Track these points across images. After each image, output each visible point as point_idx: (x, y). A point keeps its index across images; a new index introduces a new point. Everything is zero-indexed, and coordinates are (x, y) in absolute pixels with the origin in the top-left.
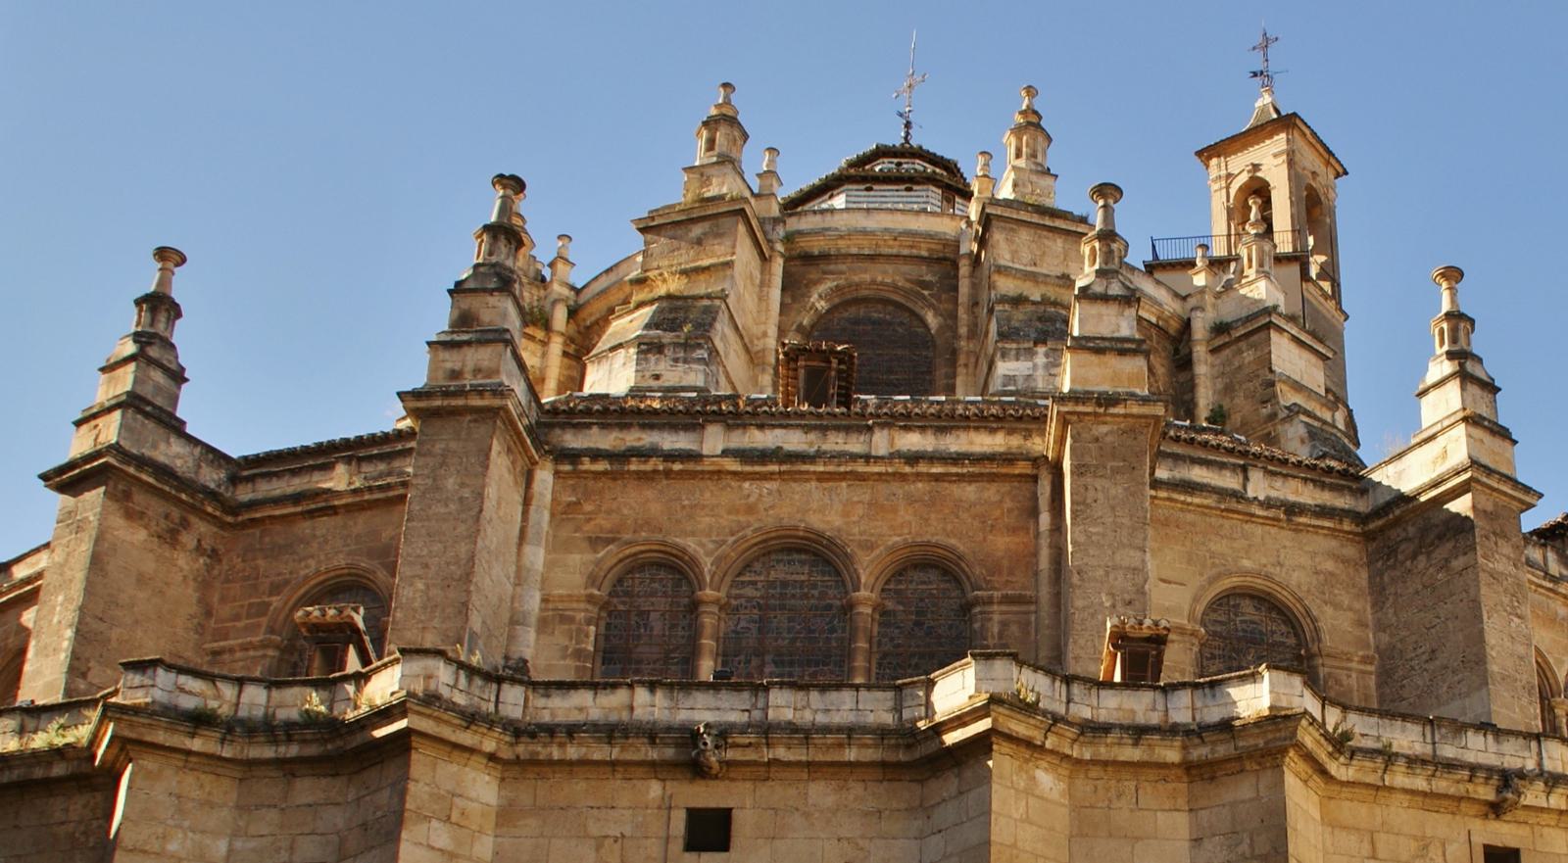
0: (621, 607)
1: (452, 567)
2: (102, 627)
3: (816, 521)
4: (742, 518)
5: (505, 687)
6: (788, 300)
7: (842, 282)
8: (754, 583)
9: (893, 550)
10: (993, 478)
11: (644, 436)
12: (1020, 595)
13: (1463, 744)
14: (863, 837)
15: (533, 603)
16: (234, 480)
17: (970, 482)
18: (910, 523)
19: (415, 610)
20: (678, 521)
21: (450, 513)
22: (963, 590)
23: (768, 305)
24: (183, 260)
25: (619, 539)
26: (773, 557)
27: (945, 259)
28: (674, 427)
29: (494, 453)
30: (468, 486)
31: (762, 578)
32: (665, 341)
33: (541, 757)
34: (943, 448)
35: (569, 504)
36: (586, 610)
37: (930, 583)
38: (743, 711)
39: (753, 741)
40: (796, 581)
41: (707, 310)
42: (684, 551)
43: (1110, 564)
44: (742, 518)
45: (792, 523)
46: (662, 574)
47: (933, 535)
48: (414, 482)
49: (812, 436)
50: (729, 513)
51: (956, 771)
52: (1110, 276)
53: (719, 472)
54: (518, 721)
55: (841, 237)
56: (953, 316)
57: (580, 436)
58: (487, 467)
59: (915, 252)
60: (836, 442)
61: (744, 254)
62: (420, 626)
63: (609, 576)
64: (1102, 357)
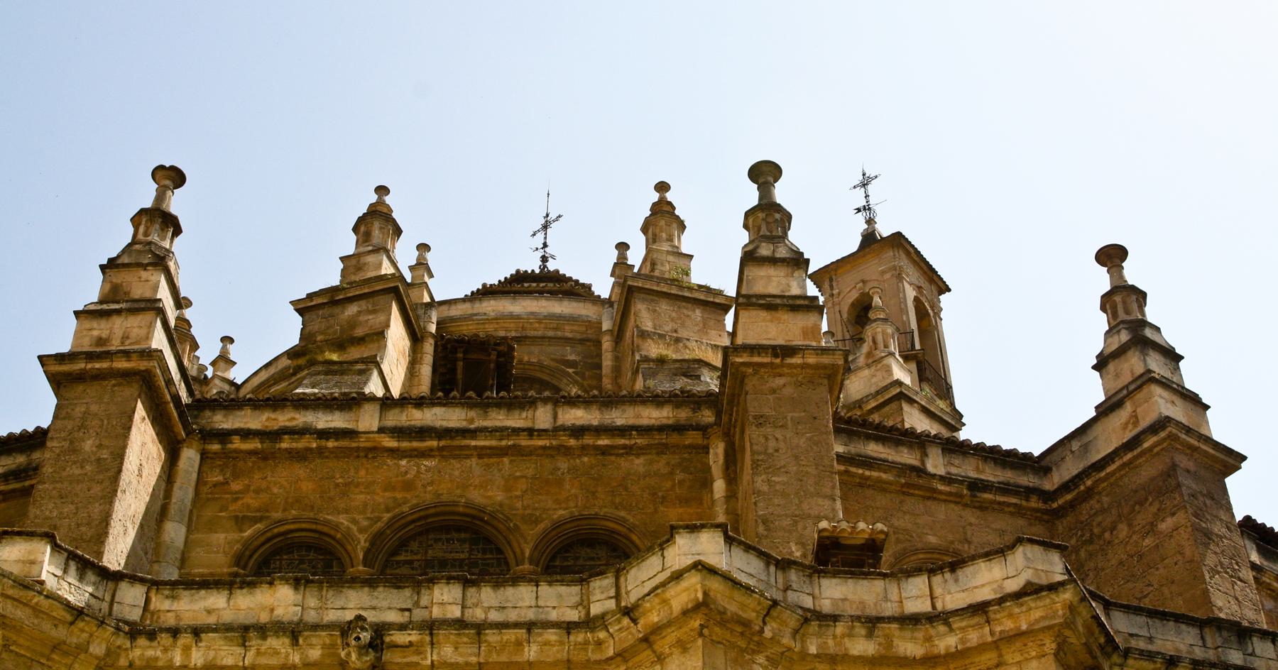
3: (476, 496)
4: (399, 495)
5: (124, 585)
8: (410, 562)
9: (558, 525)
10: (663, 449)
11: (297, 416)
17: (638, 456)
18: (576, 496)
20: (331, 499)
21: (86, 474)
25: (268, 518)
26: (431, 536)
27: (589, 340)
30: (108, 447)
31: (419, 557)
34: (609, 421)
37: (599, 559)
40: (455, 560)
42: (337, 527)
43: (797, 512)
44: (399, 495)
45: (452, 499)
46: (312, 555)
47: (601, 508)
49: (472, 414)
50: (385, 490)
52: (776, 241)
53: (374, 449)
59: (559, 334)
60: (499, 419)
63: (255, 557)
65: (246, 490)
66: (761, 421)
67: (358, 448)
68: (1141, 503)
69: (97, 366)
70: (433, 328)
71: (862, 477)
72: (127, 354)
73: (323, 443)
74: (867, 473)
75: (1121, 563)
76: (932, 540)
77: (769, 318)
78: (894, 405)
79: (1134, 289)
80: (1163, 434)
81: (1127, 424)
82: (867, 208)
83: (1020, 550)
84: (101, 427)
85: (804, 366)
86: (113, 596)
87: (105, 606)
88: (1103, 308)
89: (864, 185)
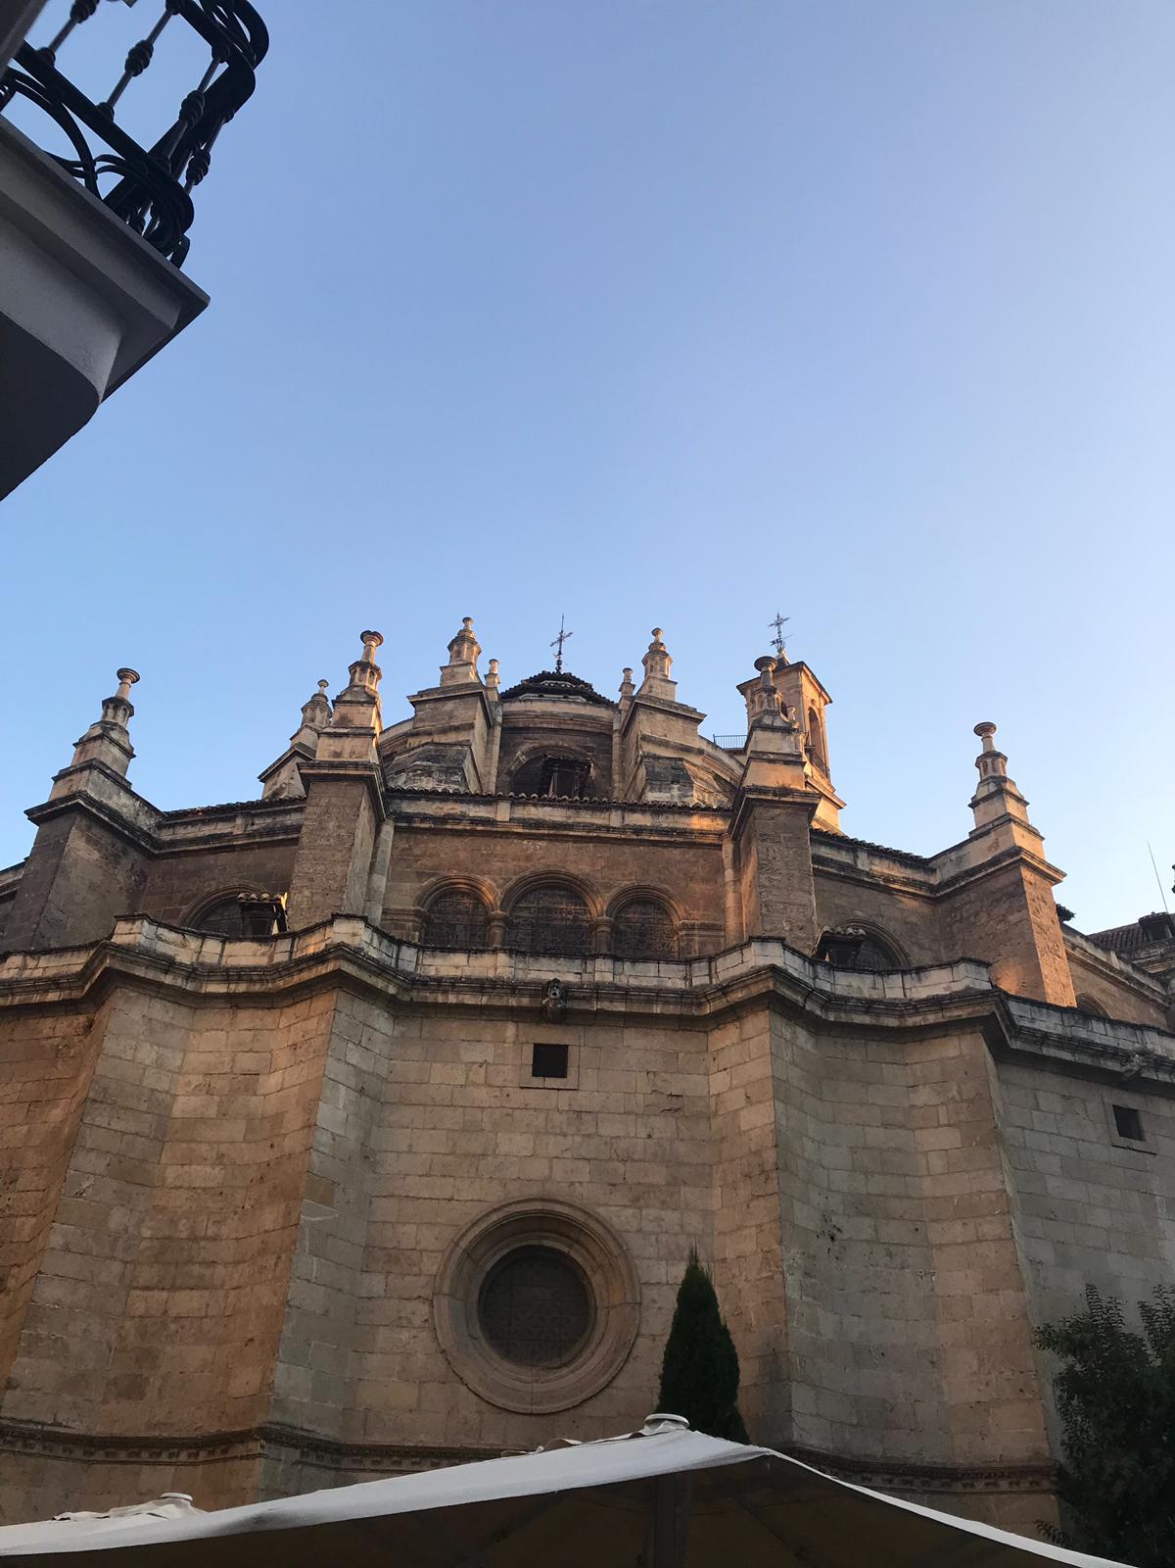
0: (436, 921)
1: (331, 882)
2: (62, 917)
3: (573, 869)
6: (502, 755)
7: (537, 745)
8: (529, 908)
9: (625, 892)
11: (456, 807)
12: (714, 925)
14: (666, 1072)
16: (159, 826)
17: (676, 848)
19: (302, 910)
22: (671, 921)
23: (491, 755)
26: (542, 892)
29: (362, 808)
30: (343, 827)
31: (534, 905)
32: (433, 769)
33: (429, 1001)
36: (414, 921)
37: (649, 914)
41: (459, 752)
44: (522, 864)
48: (306, 823)
49: (570, 813)
50: (513, 860)
51: (738, 1024)
54: (412, 973)
55: (537, 717)
56: (610, 769)
57: (413, 805)
58: (358, 816)
59: (583, 728)
60: (586, 817)
61: (480, 722)
63: (430, 899)
64: (772, 765)
65: (424, 855)
66: (764, 837)
67: (497, 832)
68: (998, 901)
70: (499, 719)
72: (356, 765)
73: (474, 827)
79: (998, 755)
82: (779, 641)
83: (962, 966)
84: (339, 813)
86: (398, 955)
88: (977, 765)
89: (778, 624)
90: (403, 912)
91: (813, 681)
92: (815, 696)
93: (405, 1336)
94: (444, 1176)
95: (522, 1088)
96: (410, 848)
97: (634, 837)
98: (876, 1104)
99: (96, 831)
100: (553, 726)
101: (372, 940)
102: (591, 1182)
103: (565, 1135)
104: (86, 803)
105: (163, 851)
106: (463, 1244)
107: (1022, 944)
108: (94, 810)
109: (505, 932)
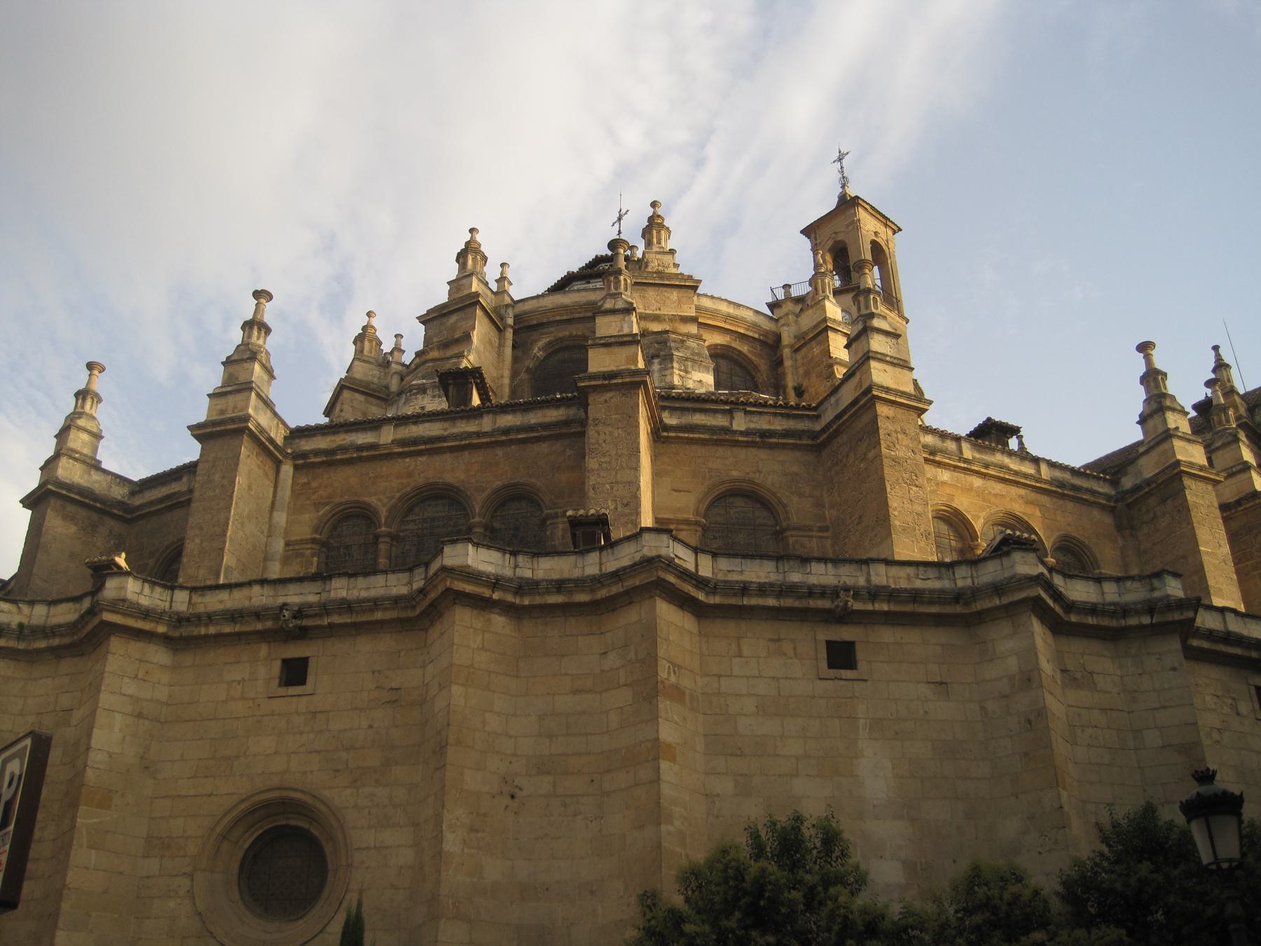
0: (335, 545)
3: (449, 478)
7: (552, 338)
8: (415, 521)
10: (558, 437)
13: (808, 571)
15: (279, 545)
21: (216, 496)
24: (102, 370)
28: (365, 430)
35: (304, 484)
36: (312, 548)
38: (317, 594)
39: (317, 612)
42: (369, 505)
43: (613, 481)
49: (447, 425)
52: (616, 296)
62: (197, 565)
69: (218, 429)
70: (510, 321)
71: (688, 438)
74: (691, 436)
75: (850, 478)
76: (735, 473)
77: (606, 352)
78: (824, 335)
80: (869, 396)
81: (857, 386)
85: (623, 384)
86: (172, 598)
87: (167, 605)
89: (840, 160)
90: (302, 542)
91: (873, 212)
92: (881, 229)
93: (172, 904)
94: (206, 777)
95: (270, 698)
96: (309, 483)
97: (504, 438)
98: (567, 674)
99: (71, 508)
100: (565, 317)
101: (142, 589)
102: (320, 770)
103: (301, 733)
104: (55, 487)
105: (134, 515)
106: (218, 830)
107: (876, 480)
108: (64, 492)
109: (391, 546)
